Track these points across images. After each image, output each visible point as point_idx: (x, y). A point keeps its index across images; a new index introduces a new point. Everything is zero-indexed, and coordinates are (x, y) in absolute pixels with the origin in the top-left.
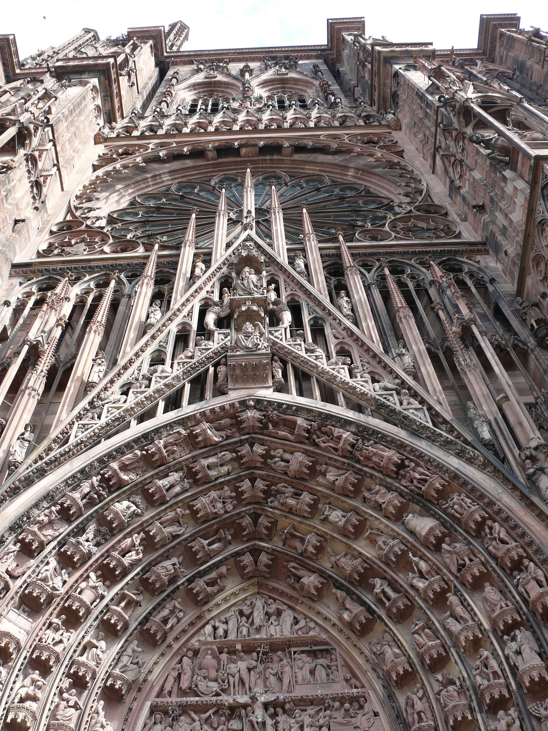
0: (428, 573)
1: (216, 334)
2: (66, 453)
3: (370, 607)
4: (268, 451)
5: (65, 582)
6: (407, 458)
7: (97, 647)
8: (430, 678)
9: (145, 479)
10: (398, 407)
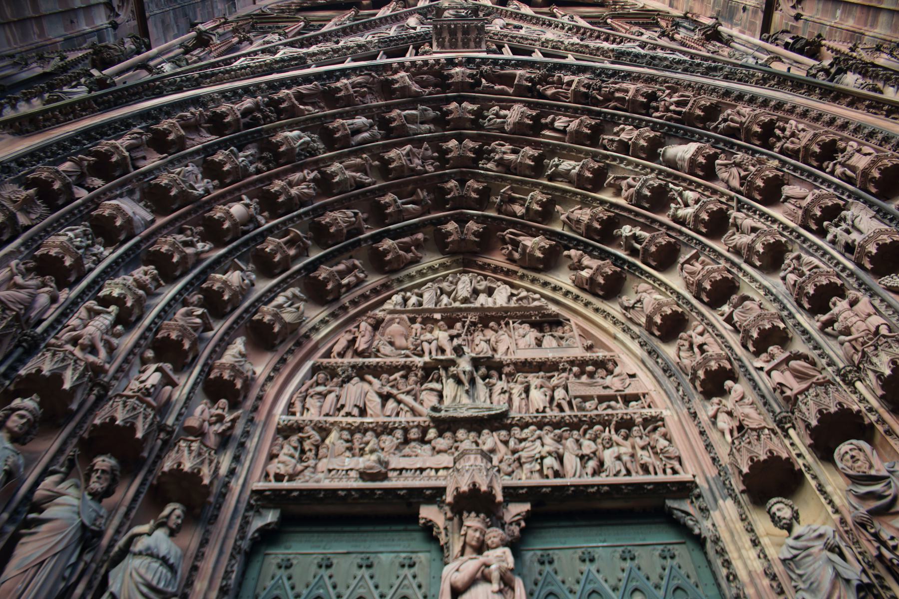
2: (227, 72)
5: (207, 192)
6: (659, 90)
7: (242, 270)
9: (325, 116)
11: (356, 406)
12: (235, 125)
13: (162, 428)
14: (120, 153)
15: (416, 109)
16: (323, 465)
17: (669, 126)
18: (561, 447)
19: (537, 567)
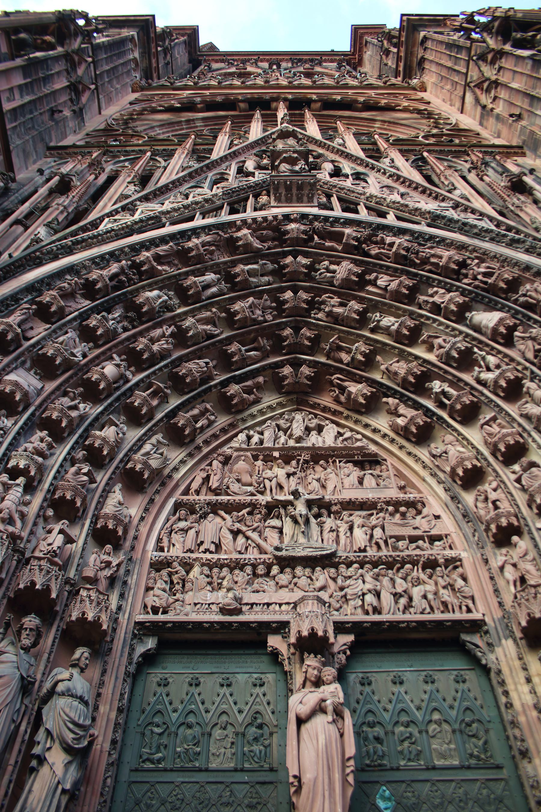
0: (498, 367)
1: (257, 173)
2: (95, 237)
4: (313, 264)
5: (84, 356)
6: (469, 258)
7: (117, 426)
9: (180, 274)
10: (456, 217)
11: (213, 542)
12: (105, 290)
13: (67, 581)
14: (14, 330)
15: (257, 263)
16: (189, 597)
17: (476, 293)
18: (378, 583)
19: (359, 688)
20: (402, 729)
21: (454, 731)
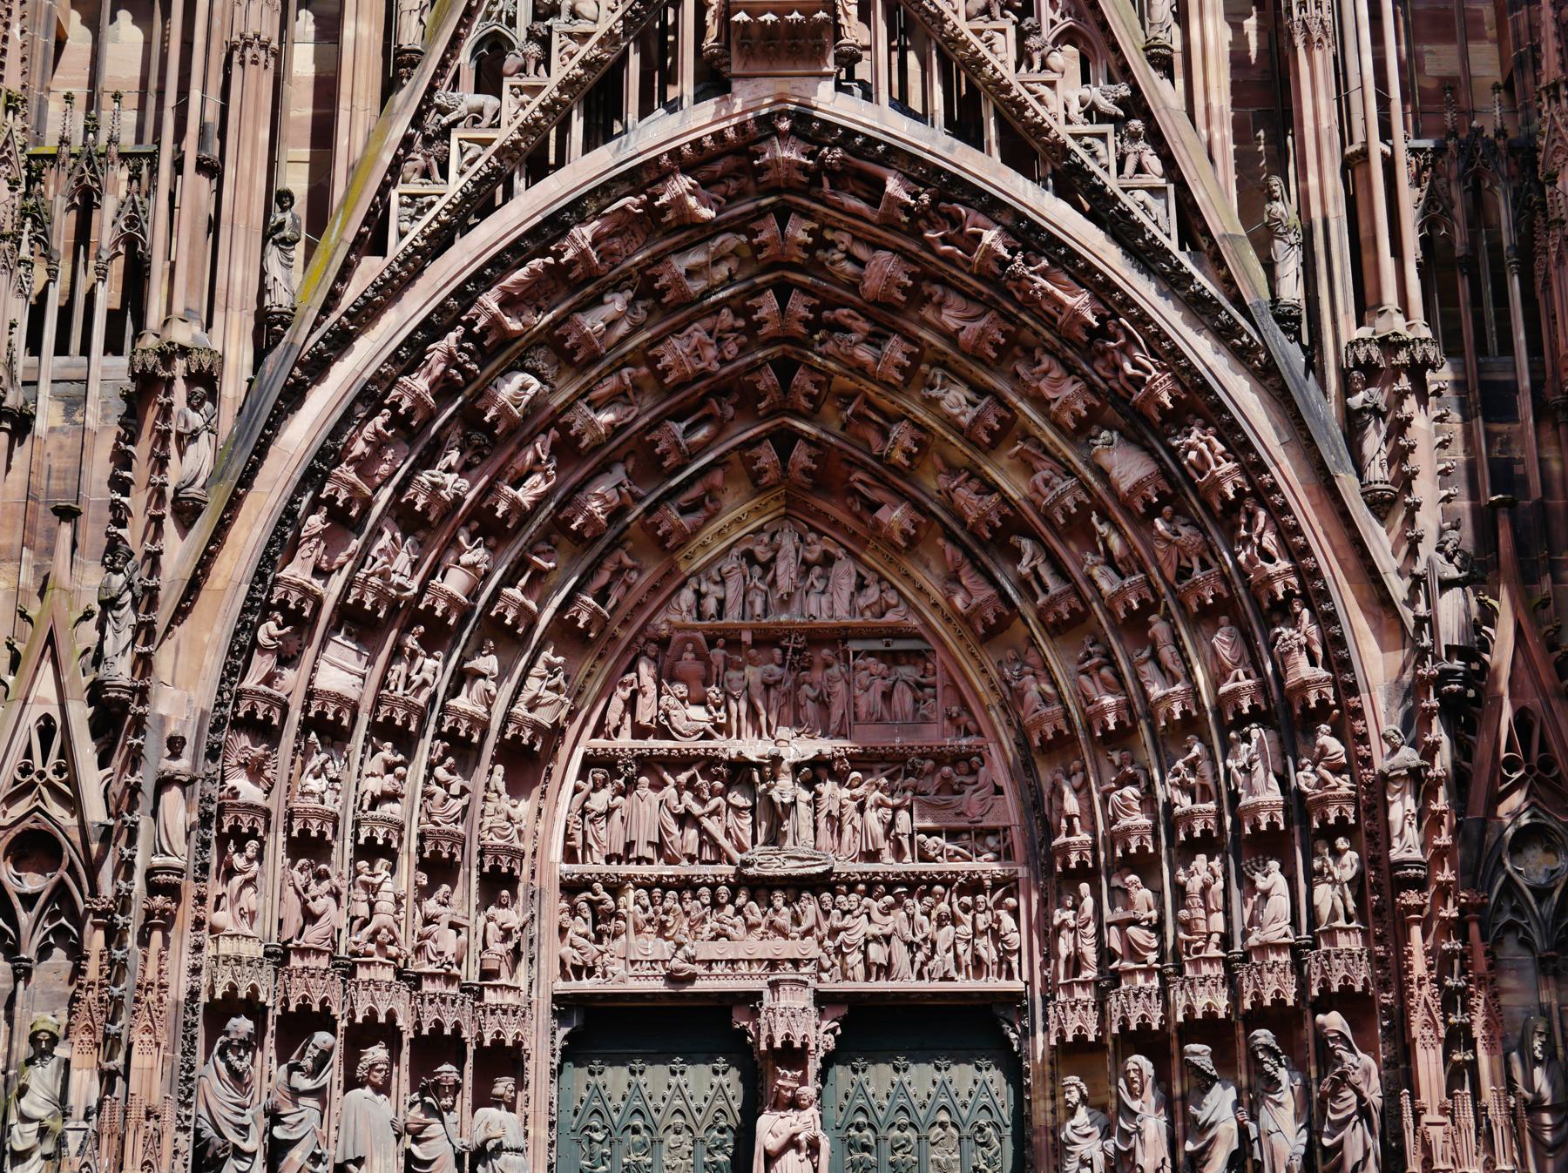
3: (1006, 593)
8: (1099, 754)
11: (650, 843)
20: (897, 1133)
21: (960, 1139)
